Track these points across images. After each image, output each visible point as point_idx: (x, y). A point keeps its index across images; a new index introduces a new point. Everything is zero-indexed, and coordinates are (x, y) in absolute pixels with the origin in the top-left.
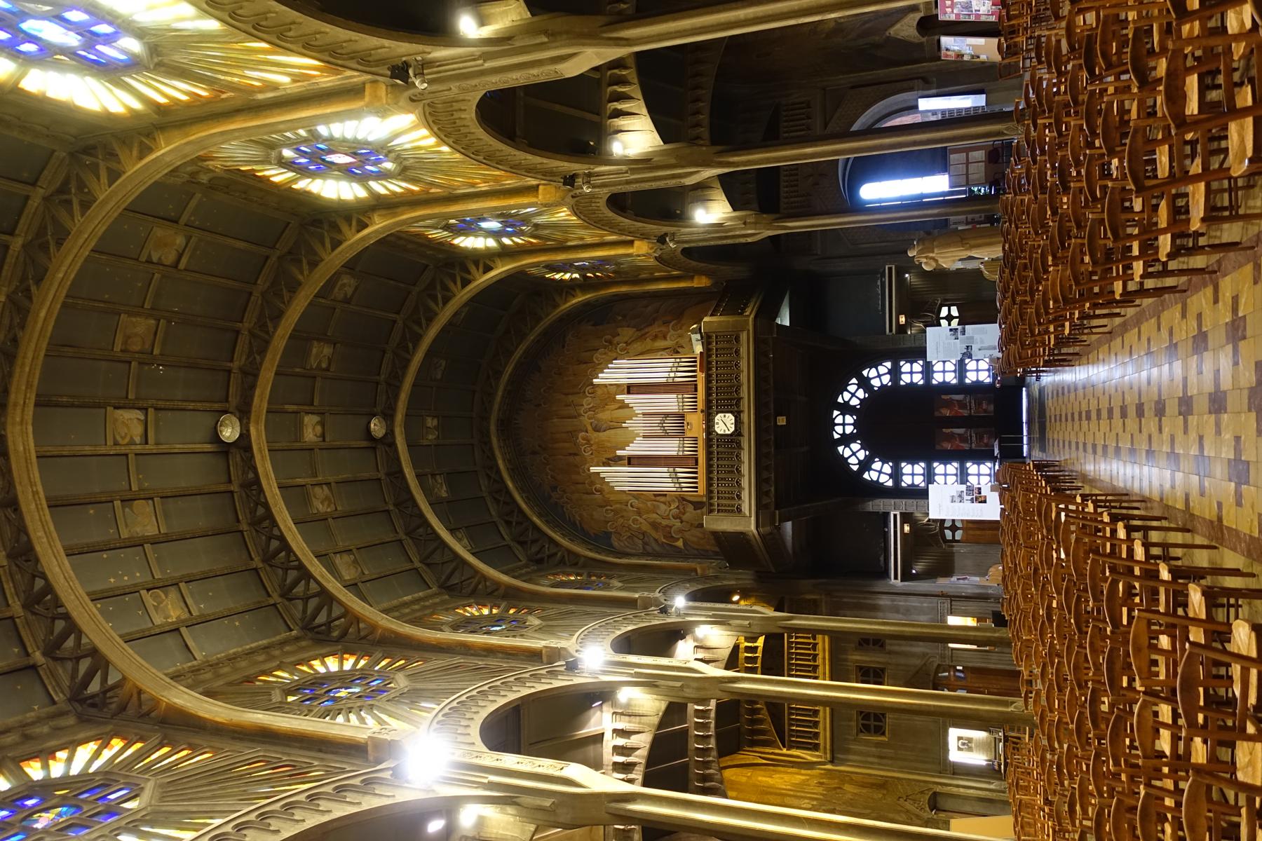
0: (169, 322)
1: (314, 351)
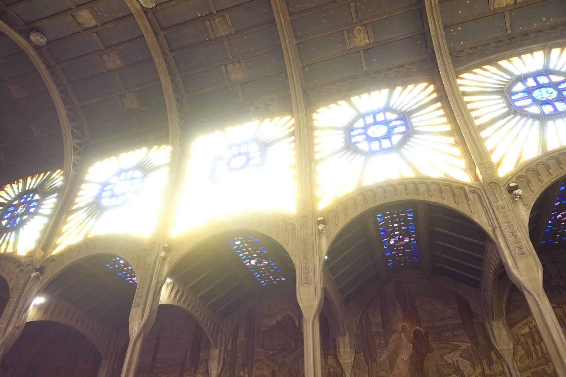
0: (210, 40)
1: (118, 62)
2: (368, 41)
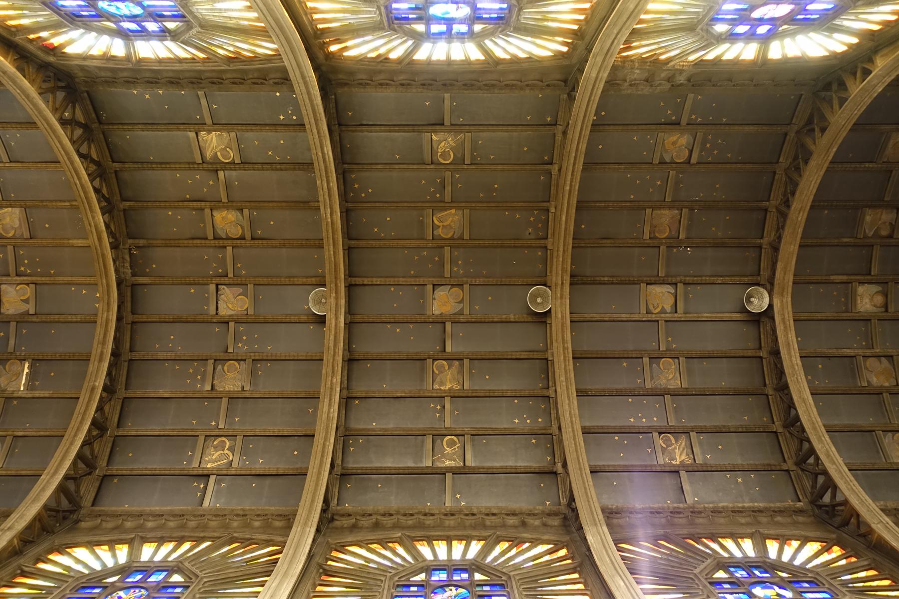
0: (692, 210)
1: (868, 218)
2: (434, 137)
